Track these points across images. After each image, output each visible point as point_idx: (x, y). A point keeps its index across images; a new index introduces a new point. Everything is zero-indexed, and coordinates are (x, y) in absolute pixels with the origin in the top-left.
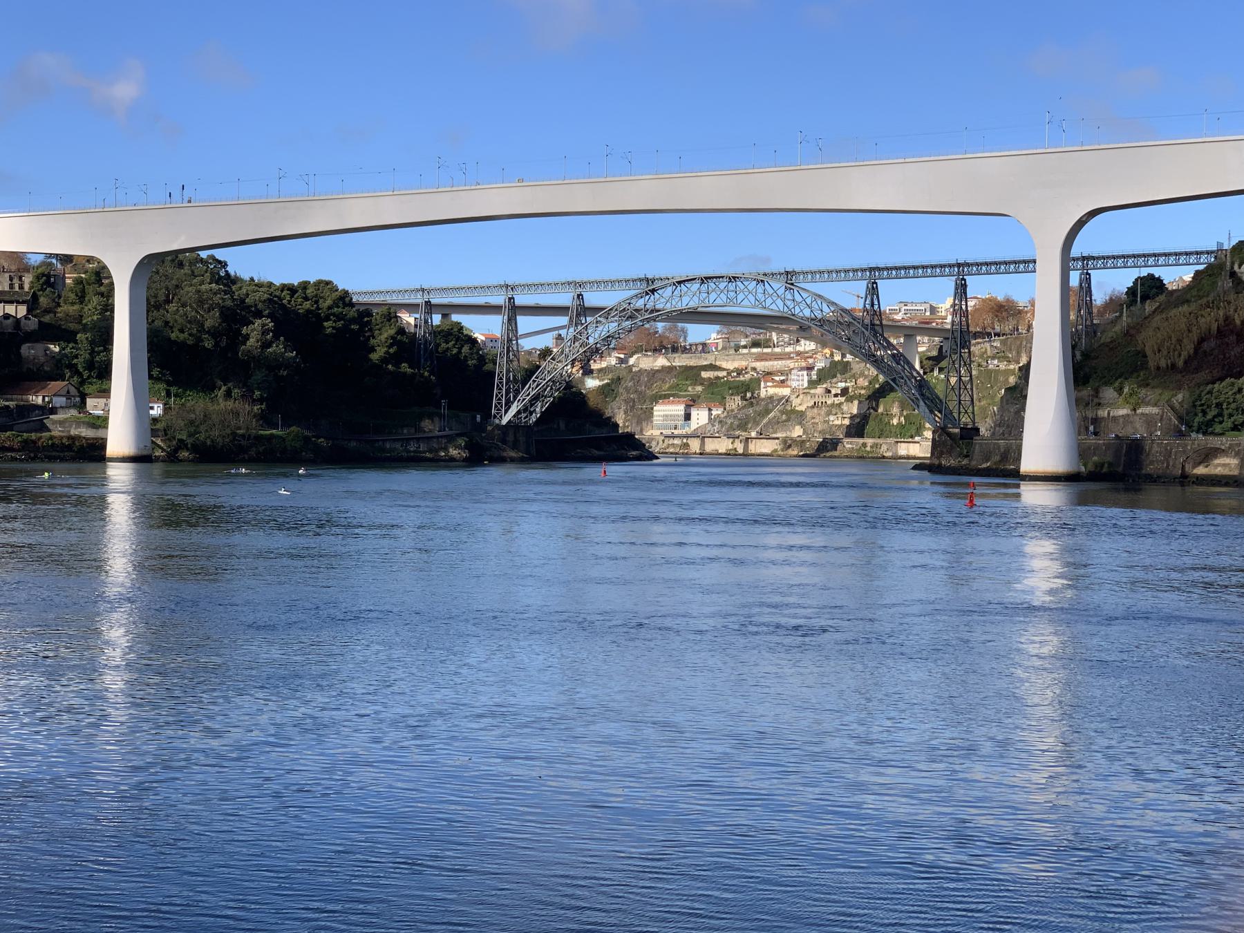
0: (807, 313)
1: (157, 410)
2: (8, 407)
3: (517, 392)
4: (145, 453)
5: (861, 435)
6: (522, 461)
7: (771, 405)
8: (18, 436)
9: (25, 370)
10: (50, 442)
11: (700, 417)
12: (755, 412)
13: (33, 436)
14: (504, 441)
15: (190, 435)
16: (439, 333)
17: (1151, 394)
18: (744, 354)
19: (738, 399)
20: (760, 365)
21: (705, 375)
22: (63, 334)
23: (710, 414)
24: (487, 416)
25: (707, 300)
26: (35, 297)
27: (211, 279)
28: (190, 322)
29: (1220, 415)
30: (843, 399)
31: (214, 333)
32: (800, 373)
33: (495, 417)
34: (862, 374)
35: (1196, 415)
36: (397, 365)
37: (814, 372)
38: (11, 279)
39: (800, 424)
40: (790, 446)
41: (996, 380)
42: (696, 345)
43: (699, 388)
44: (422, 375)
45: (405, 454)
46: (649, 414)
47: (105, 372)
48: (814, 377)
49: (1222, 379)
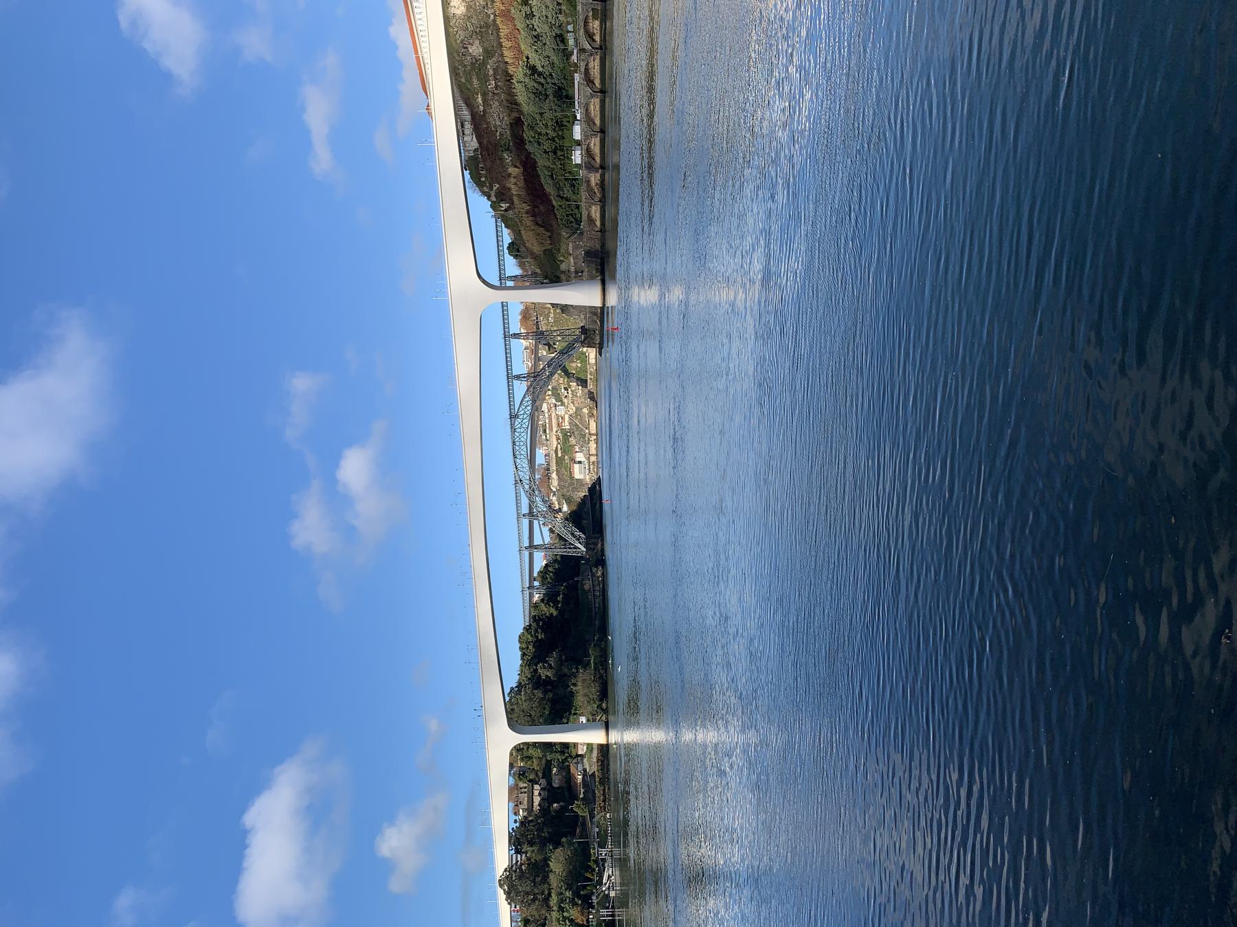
0: (529, 408)
1: (583, 719)
3: (570, 544)
5: (587, 380)
6: (603, 541)
11: (580, 457)
14: (594, 549)
15: (595, 703)
17: (563, 247)
19: (570, 439)
20: (555, 429)
21: (560, 455)
22: (549, 765)
23: (578, 452)
24: (582, 558)
29: (572, 214)
30: (569, 390)
31: (545, 692)
36: (558, 602)
38: (522, 793)
39: (581, 409)
43: (566, 457)
44: (563, 590)
45: (601, 598)
47: (565, 746)
48: (560, 403)
49: (555, 214)
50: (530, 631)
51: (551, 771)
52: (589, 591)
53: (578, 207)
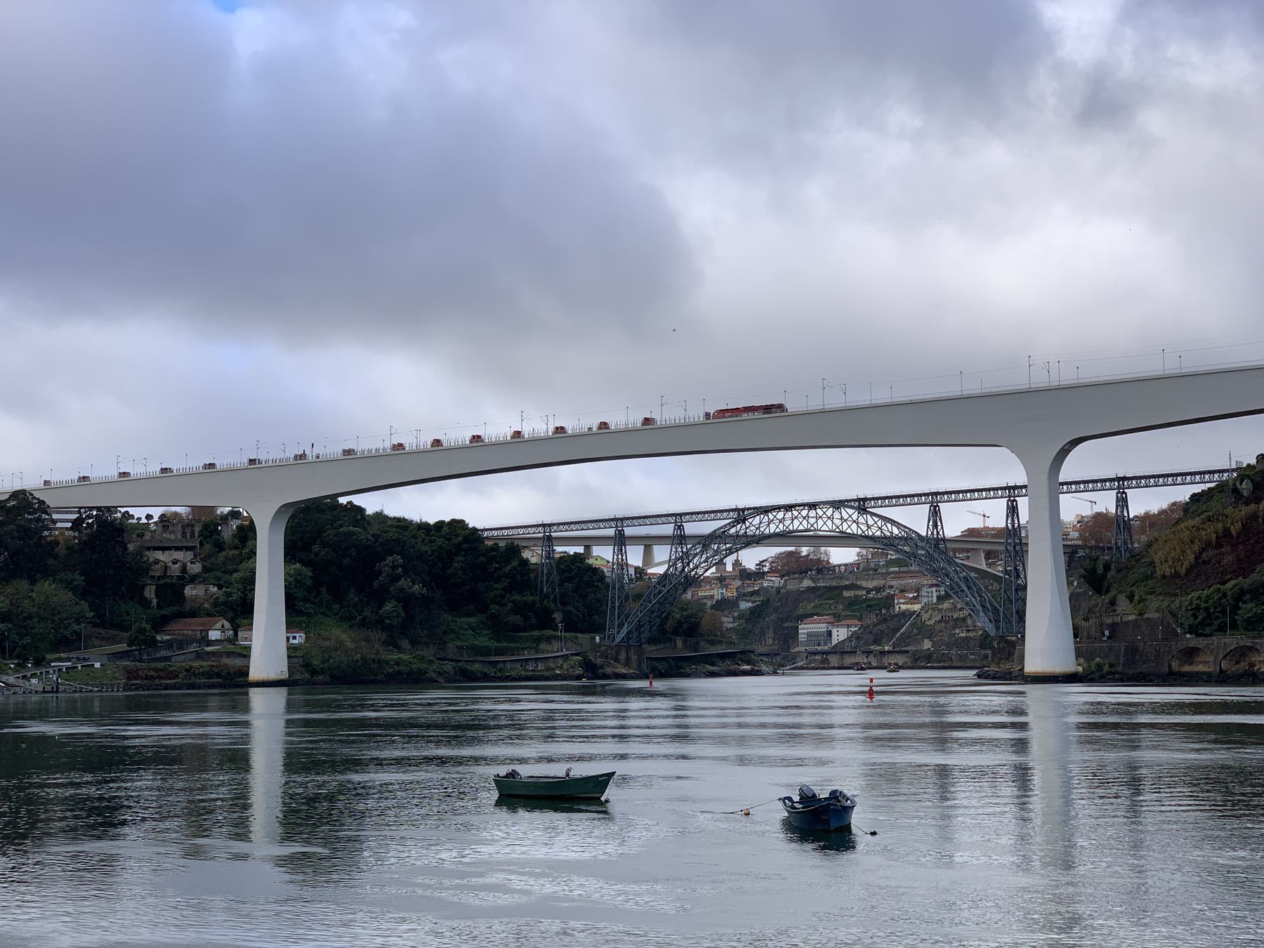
0: (878, 533)
7: (902, 621)
9: (187, 609)
12: (888, 627)
14: (617, 660)
21: (846, 594)
25: (791, 526)
32: (930, 590)
39: (929, 638)
45: (523, 673)
53: (1221, 629)
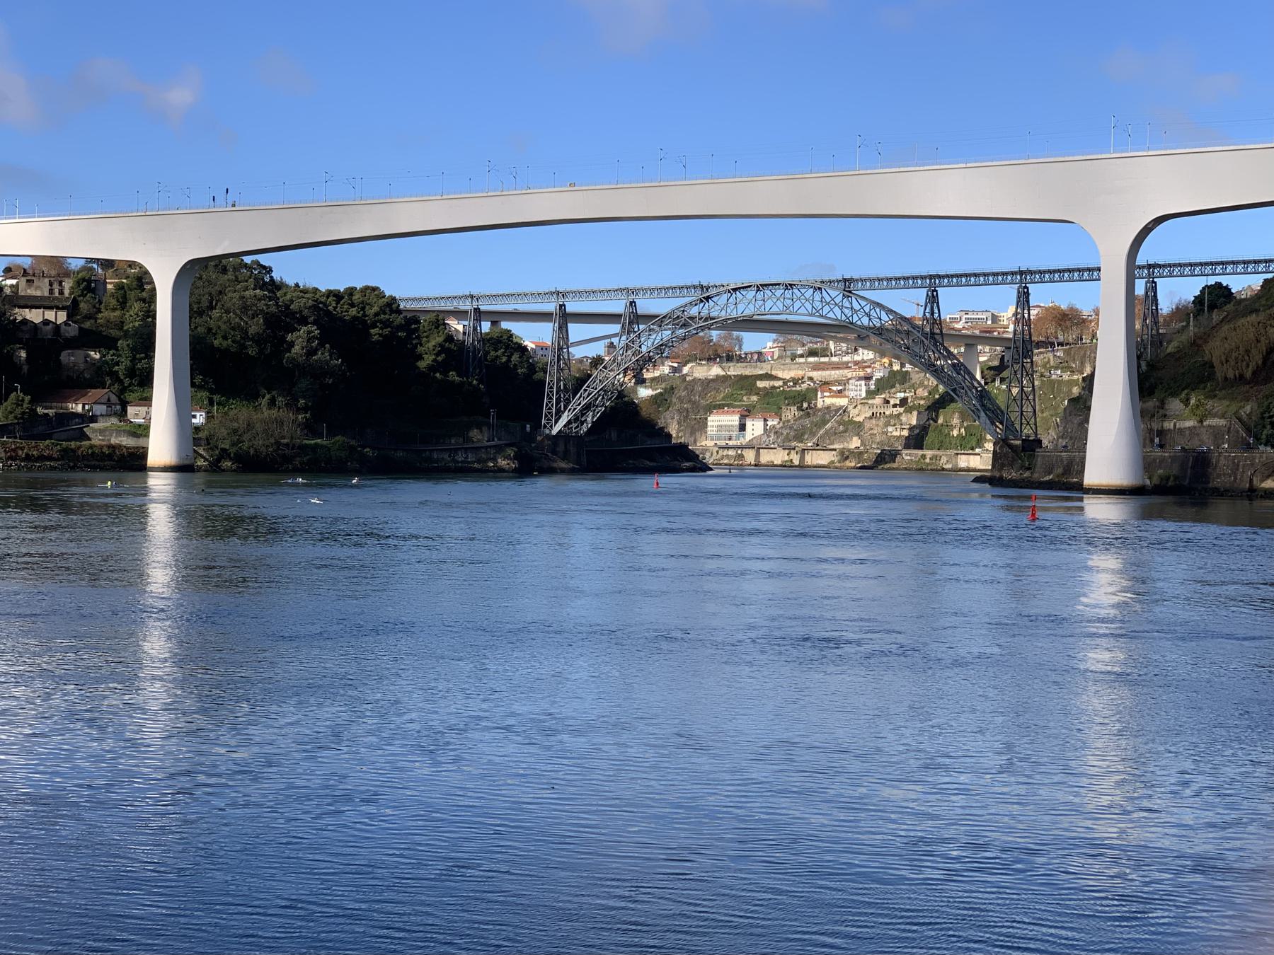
0: (865, 321)
1: (199, 419)
2: (47, 415)
3: (568, 402)
4: (187, 462)
6: (572, 472)
7: (827, 416)
8: (58, 444)
10: (90, 451)
11: (755, 428)
12: (812, 422)
13: (73, 444)
14: (554, 452)
15: (233, 444)
16: (488, 340)
18: (801, 363)
19: (794, 409)
20: (817, 375)
21: (760, 384)
22: (106, 342)
23: (766, 425)
24: (537, 426)
26: (75, 303)
27: (255, 285)
28: (233, 329)
30: (901, 410)
31: (258, 340)
32: (858, 383)
33: (545, 427)
34: (922, 384)
35: (1264, 427)
36: (445, 373)
37: (872, 382)
39: (858, 435)
40: (847, 458)
41: (1060, 391)
42: (752, 354)
43: (755, 398)
44: (470, 384)
46: (703, 425)
47: (145, 379)
48: (873, 387)
50: (387, 310)
51: (94, 348)
52: (469, 440)
